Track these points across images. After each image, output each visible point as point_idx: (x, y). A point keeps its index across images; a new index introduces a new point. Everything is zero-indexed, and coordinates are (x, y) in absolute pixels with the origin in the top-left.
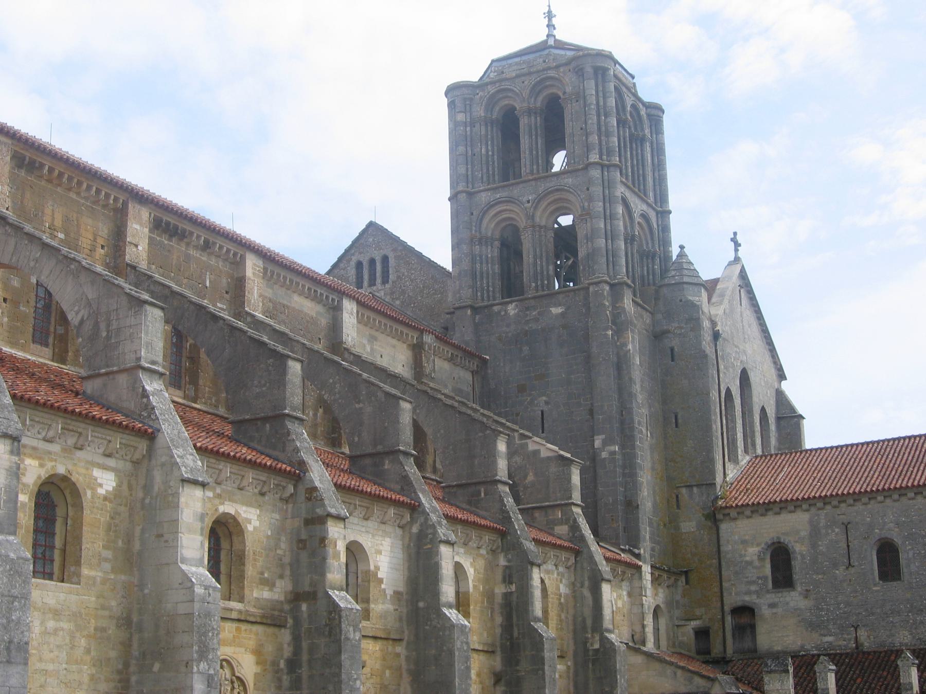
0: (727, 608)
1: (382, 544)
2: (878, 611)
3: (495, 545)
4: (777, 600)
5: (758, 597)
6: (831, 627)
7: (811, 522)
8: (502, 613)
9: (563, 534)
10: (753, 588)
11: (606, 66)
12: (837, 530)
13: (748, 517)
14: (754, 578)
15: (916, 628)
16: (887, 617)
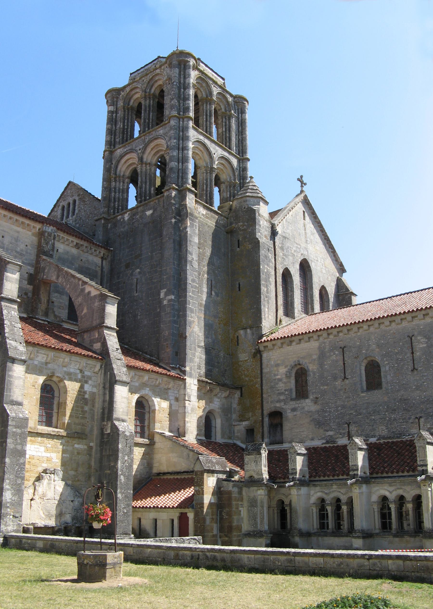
0: (266, 412)
2: (364, 411)
4: (297, 405)
5: (285, 404)
6: (332, 424)
7: (319, 348)
10: (282, 397)
12: (337, 352)
14: (283, 391)
15: (391, 424)
16: (370, 416)
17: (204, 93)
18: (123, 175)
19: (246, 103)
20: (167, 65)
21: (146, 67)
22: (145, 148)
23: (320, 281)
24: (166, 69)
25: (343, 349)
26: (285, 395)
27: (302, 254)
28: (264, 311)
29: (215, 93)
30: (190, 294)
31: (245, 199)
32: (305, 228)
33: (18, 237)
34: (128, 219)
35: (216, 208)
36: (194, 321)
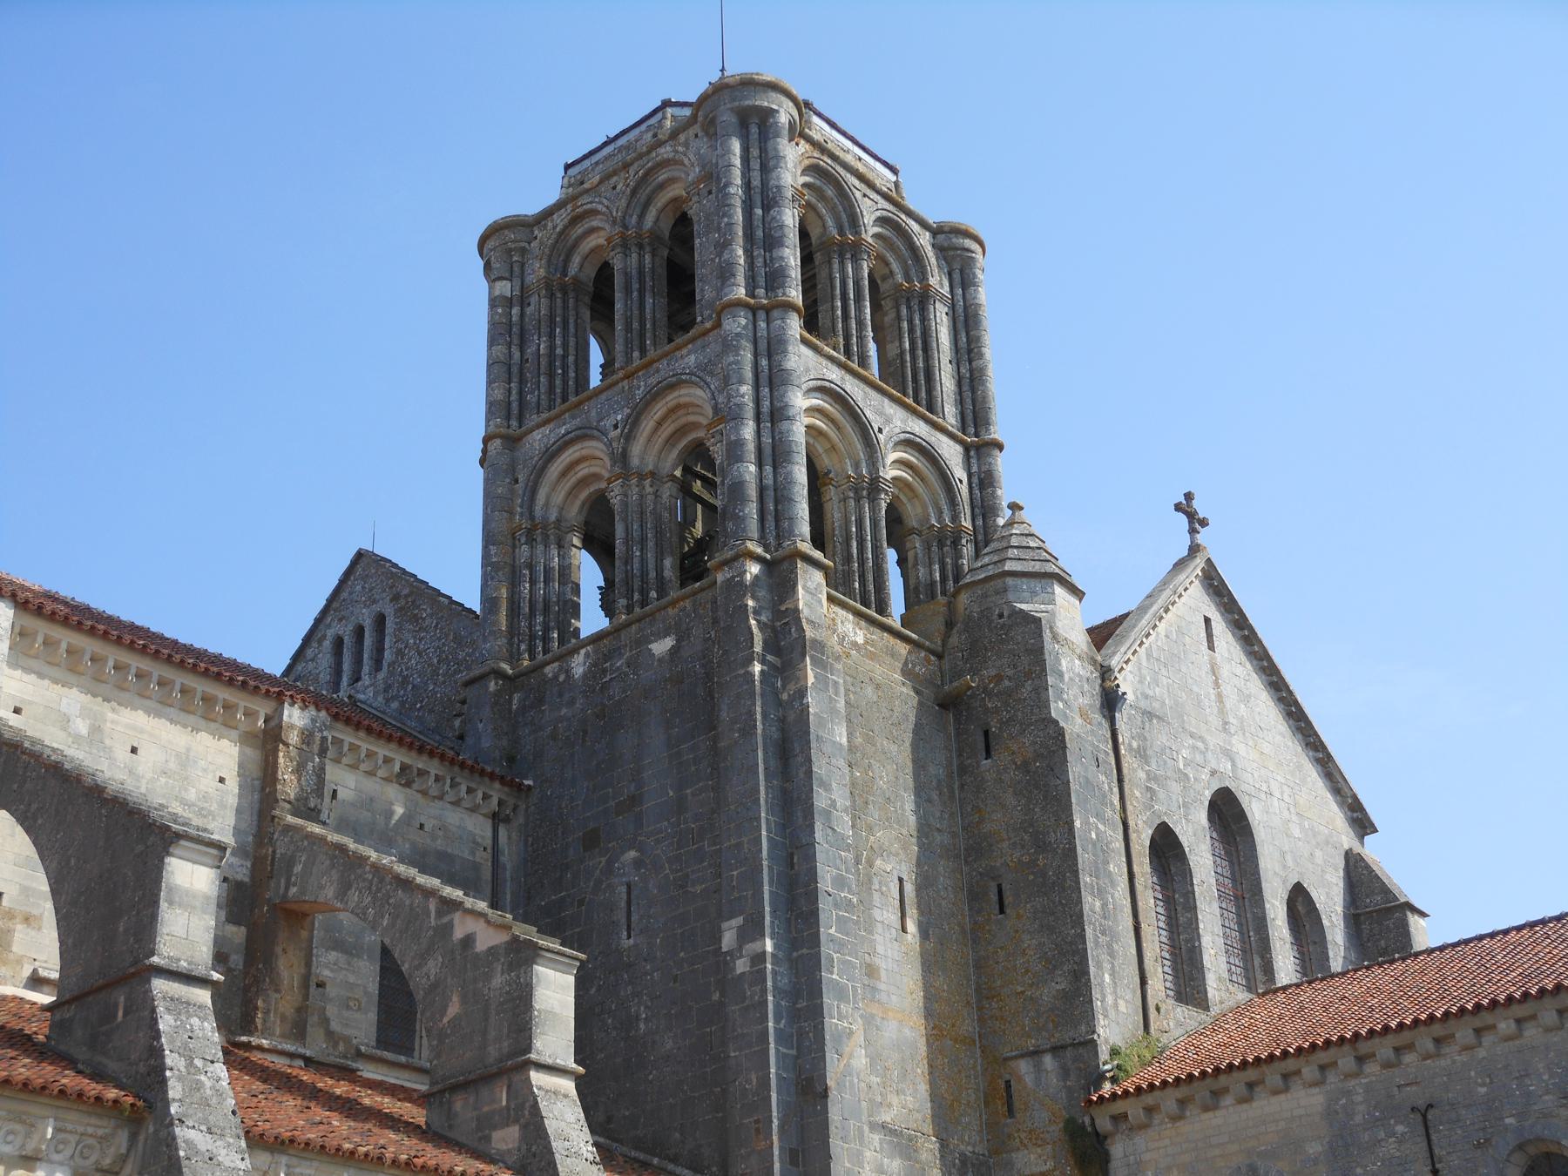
7: (1329, 1113)
11: (766, 104)
12: (1400, 1128)
17: (830, 222)
18: (558, 520)
19: (975, 246)
20: (696, 128)
21: (622, 141)
22: (634, 421)
23: (1285, 867)
24: (694, 144)
25: (1424, 1113)
27: (1213, 773)
28: (1101, 984)
29: (868, 218)
30: (832, 931)
31: (998, 583)
32: (1217, 679)
33: (188, 750)
34: (585, 675)
35: (895, 621)
36: (851, 1033)
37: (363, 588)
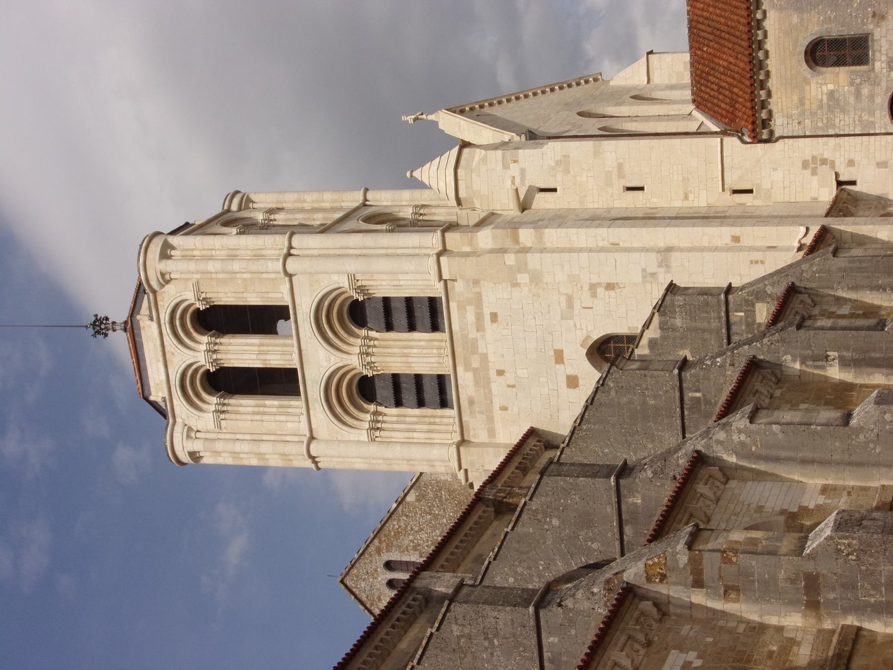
1: (749, 505)
3: (769, 377)
5: (879, 84)
7: (781, 9)
8: (869, 375)
9: (768, 310)
13: (769, 94)
14: (852, 89)
26: (861, 84)
37: (364, 580)
